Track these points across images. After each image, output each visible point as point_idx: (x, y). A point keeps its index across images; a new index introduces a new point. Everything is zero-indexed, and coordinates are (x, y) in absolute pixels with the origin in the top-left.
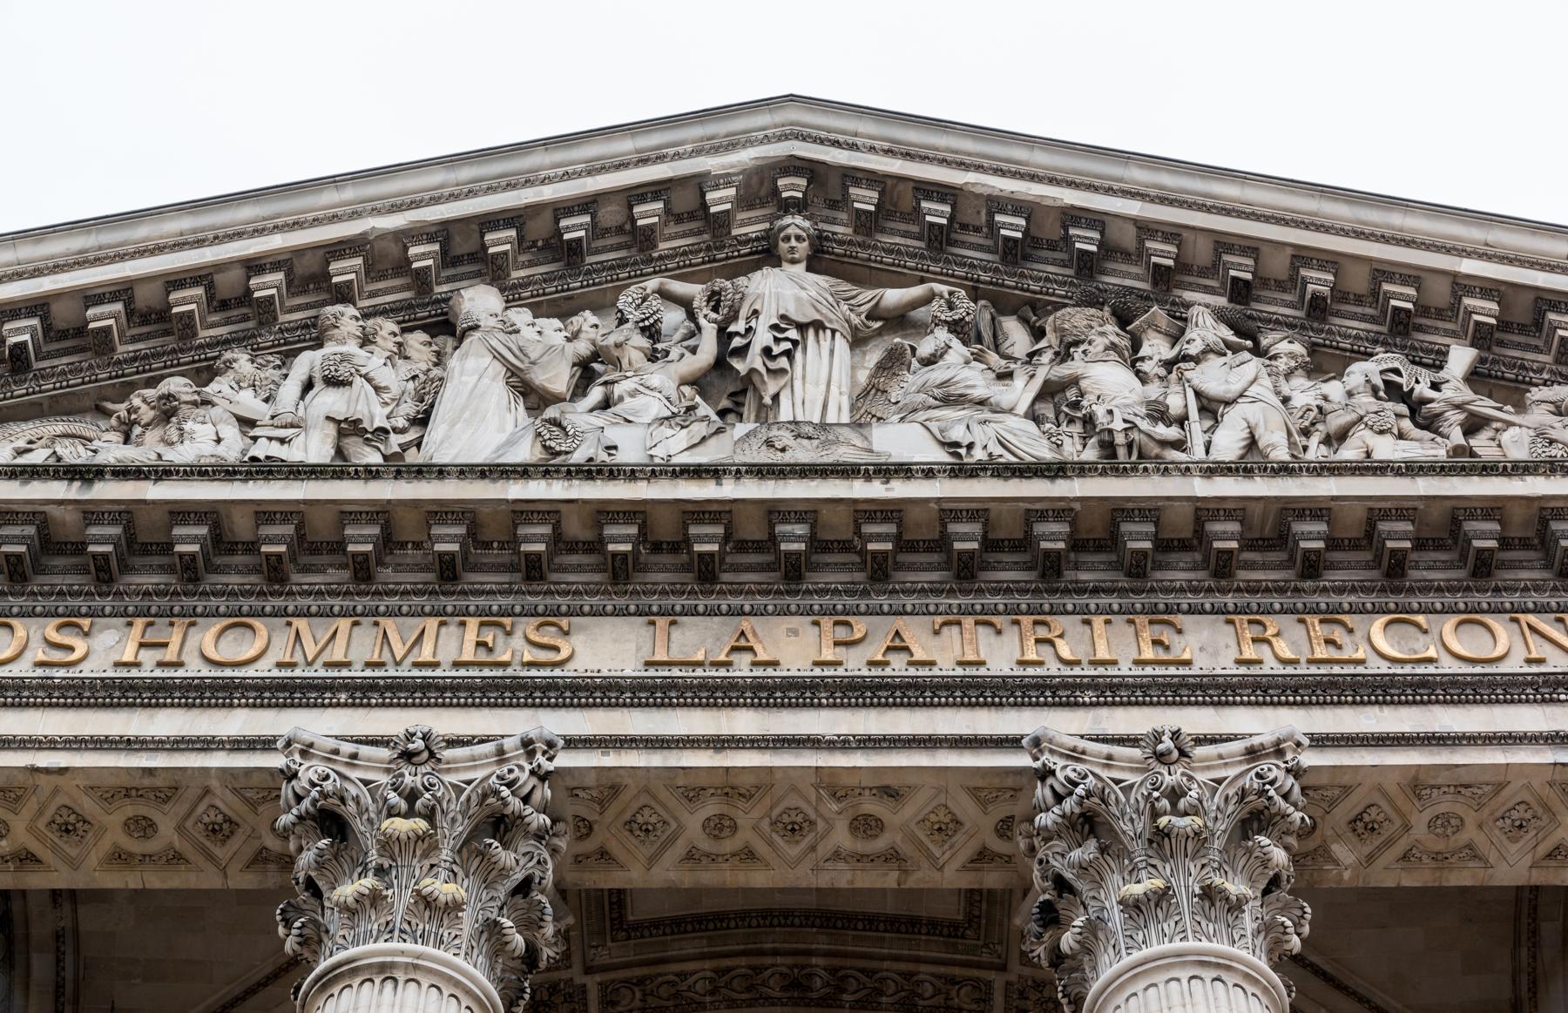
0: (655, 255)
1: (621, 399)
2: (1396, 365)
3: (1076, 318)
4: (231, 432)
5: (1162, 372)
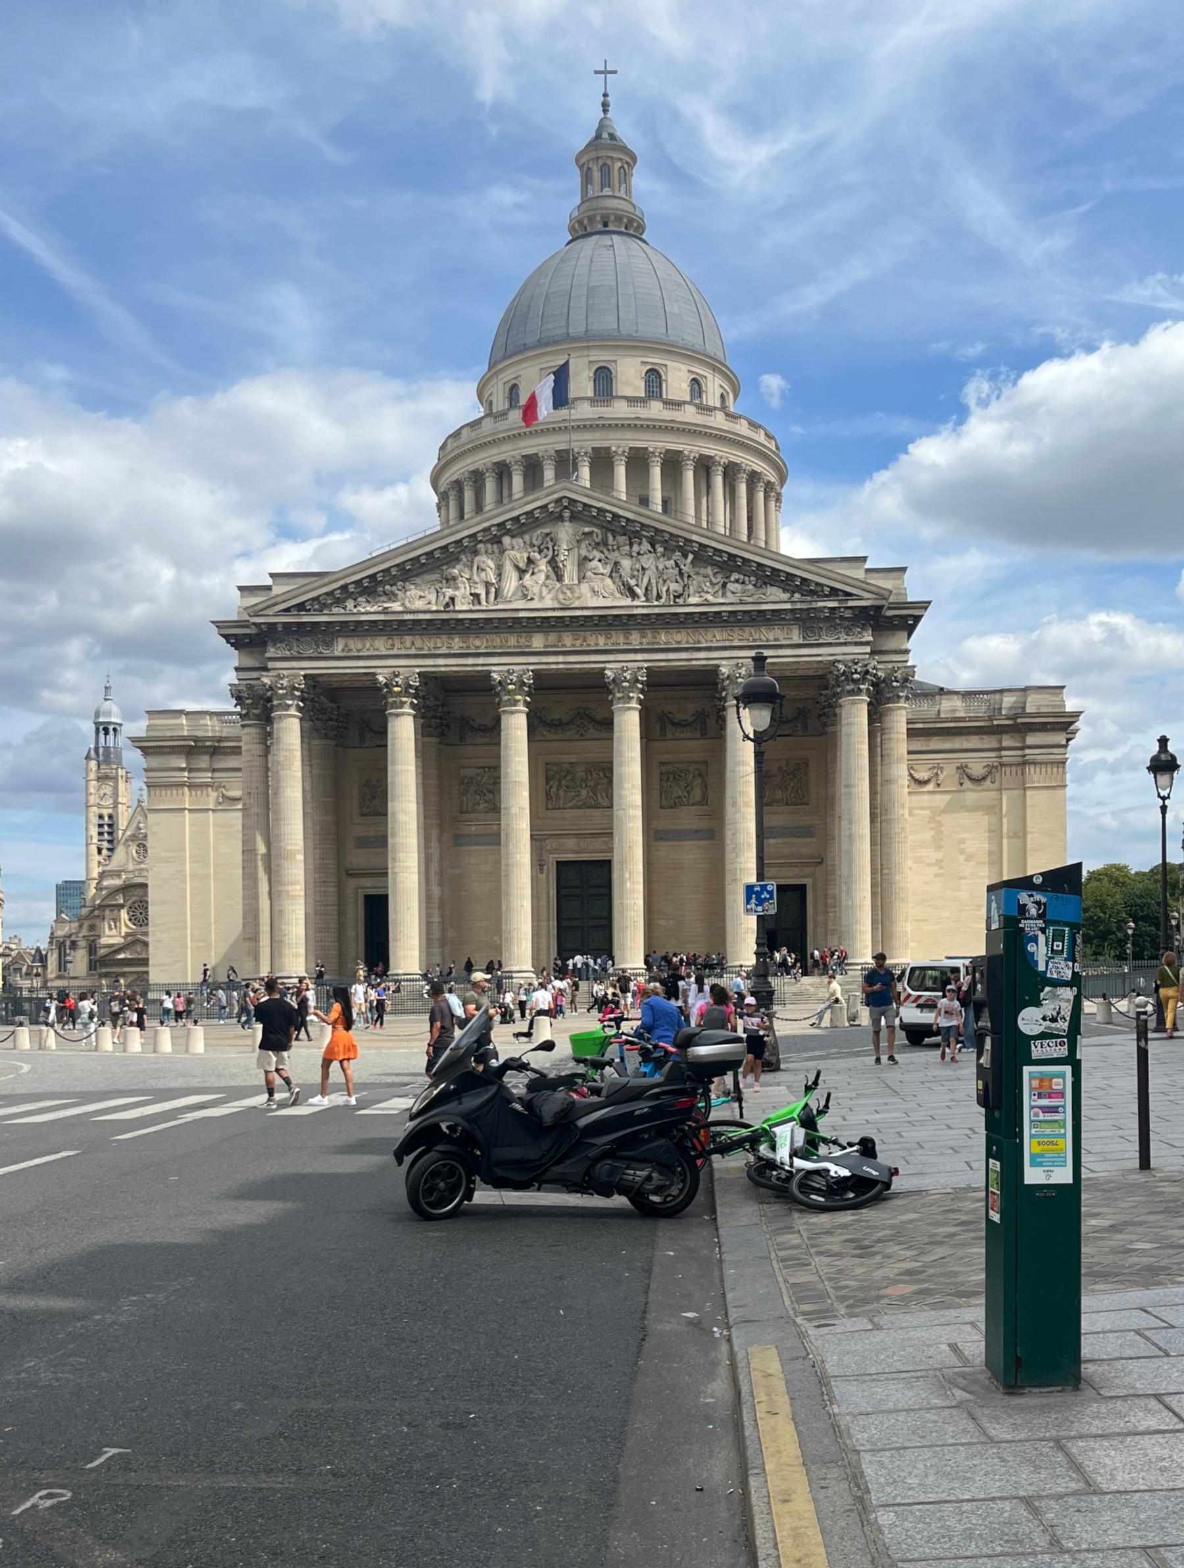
3: (622, 539)
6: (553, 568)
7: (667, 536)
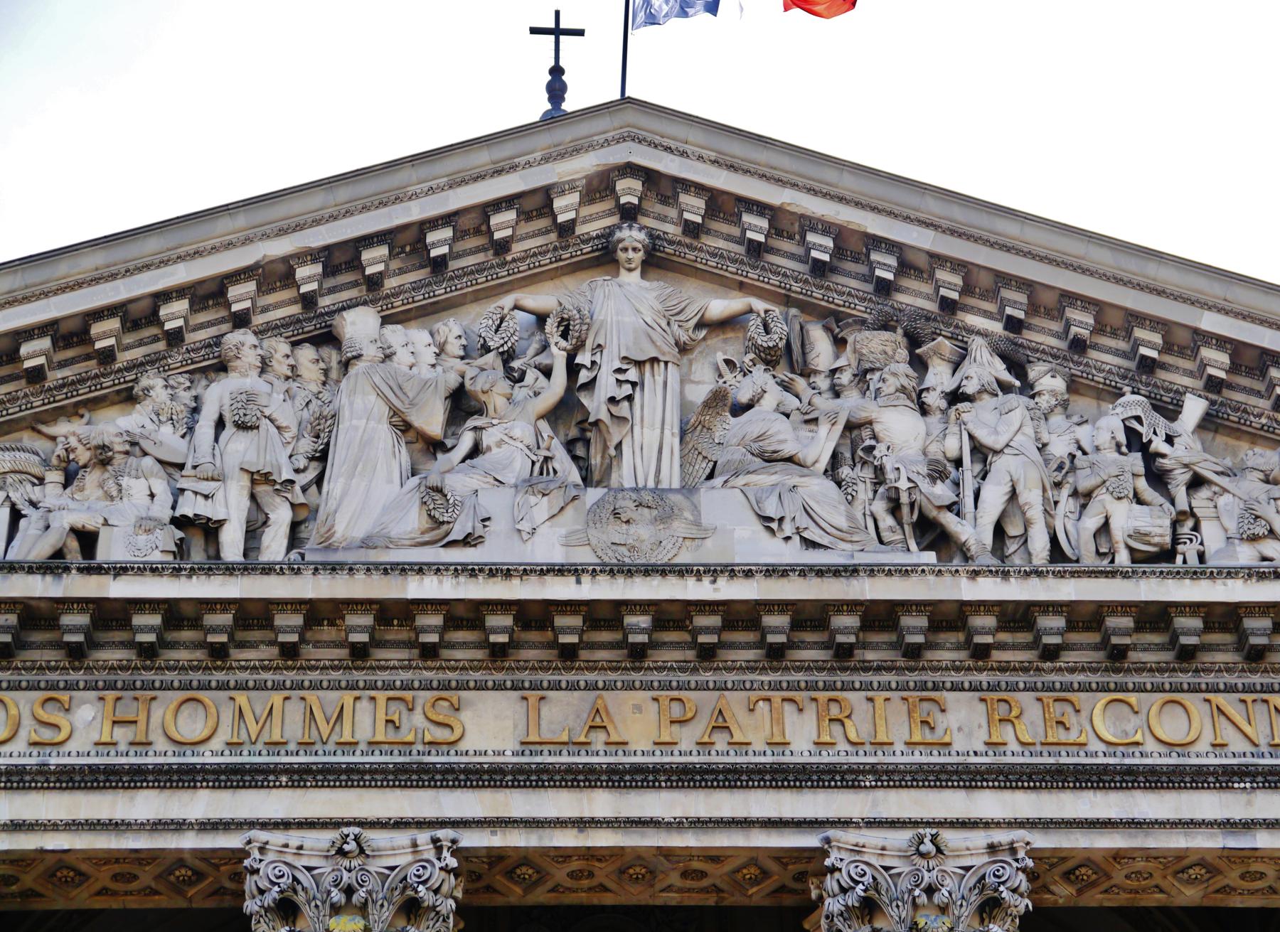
0: (509, 258)
1: (489, 449)
2: (1139, 412)
3: (875, 343)
5: (943, 404)
6: (569, 445)
7: (1082, 321)
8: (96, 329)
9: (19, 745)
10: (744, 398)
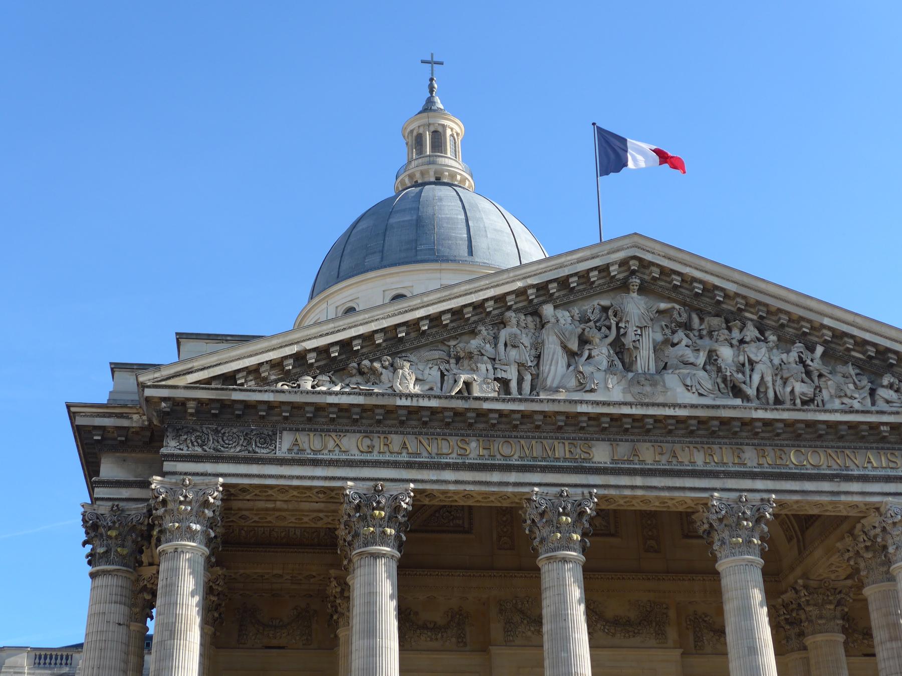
3: (716, 322)
4: (490, 367)
6: (617, 354)
8: (466, 310)
9: (454, 455)
10: (675, 341)
